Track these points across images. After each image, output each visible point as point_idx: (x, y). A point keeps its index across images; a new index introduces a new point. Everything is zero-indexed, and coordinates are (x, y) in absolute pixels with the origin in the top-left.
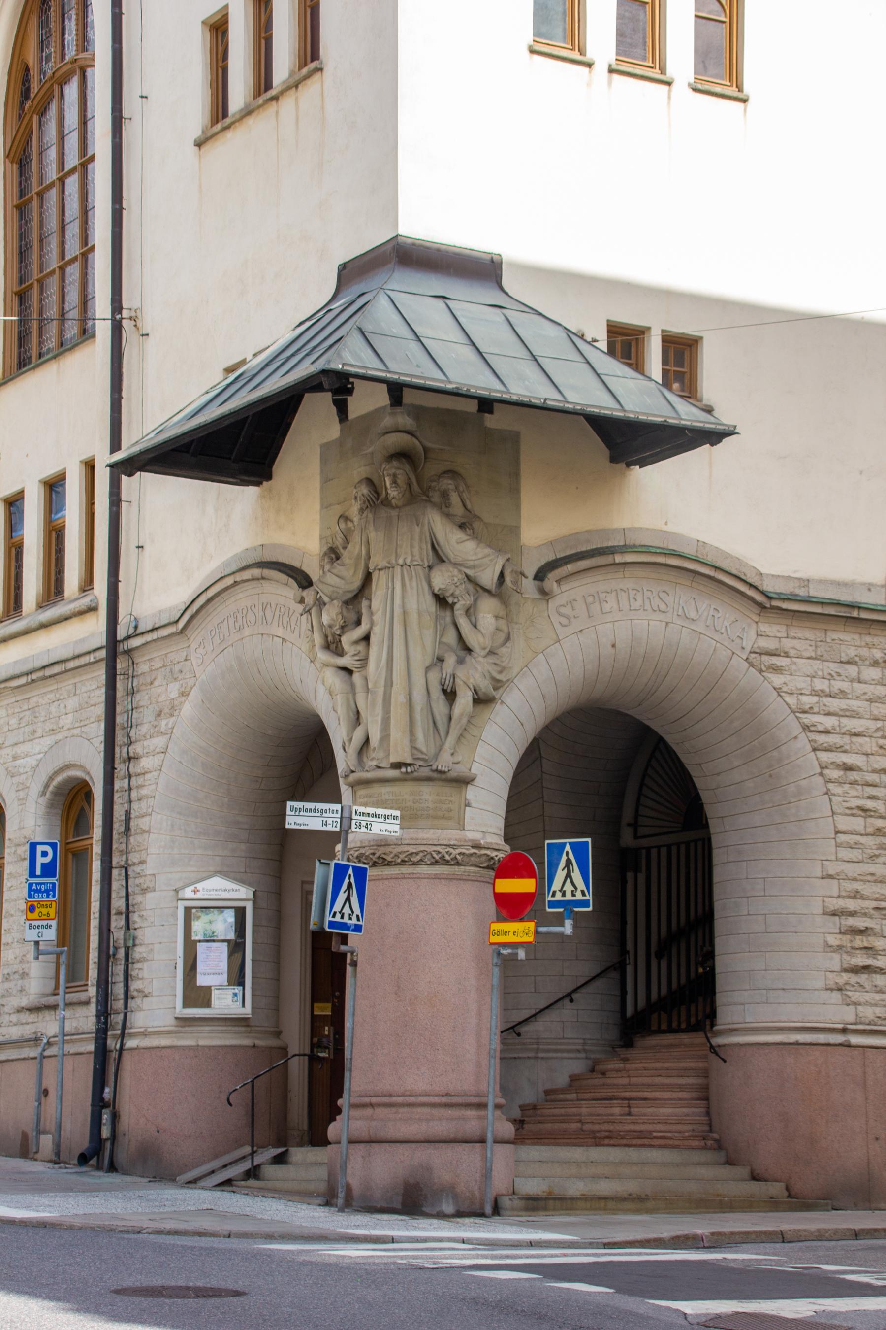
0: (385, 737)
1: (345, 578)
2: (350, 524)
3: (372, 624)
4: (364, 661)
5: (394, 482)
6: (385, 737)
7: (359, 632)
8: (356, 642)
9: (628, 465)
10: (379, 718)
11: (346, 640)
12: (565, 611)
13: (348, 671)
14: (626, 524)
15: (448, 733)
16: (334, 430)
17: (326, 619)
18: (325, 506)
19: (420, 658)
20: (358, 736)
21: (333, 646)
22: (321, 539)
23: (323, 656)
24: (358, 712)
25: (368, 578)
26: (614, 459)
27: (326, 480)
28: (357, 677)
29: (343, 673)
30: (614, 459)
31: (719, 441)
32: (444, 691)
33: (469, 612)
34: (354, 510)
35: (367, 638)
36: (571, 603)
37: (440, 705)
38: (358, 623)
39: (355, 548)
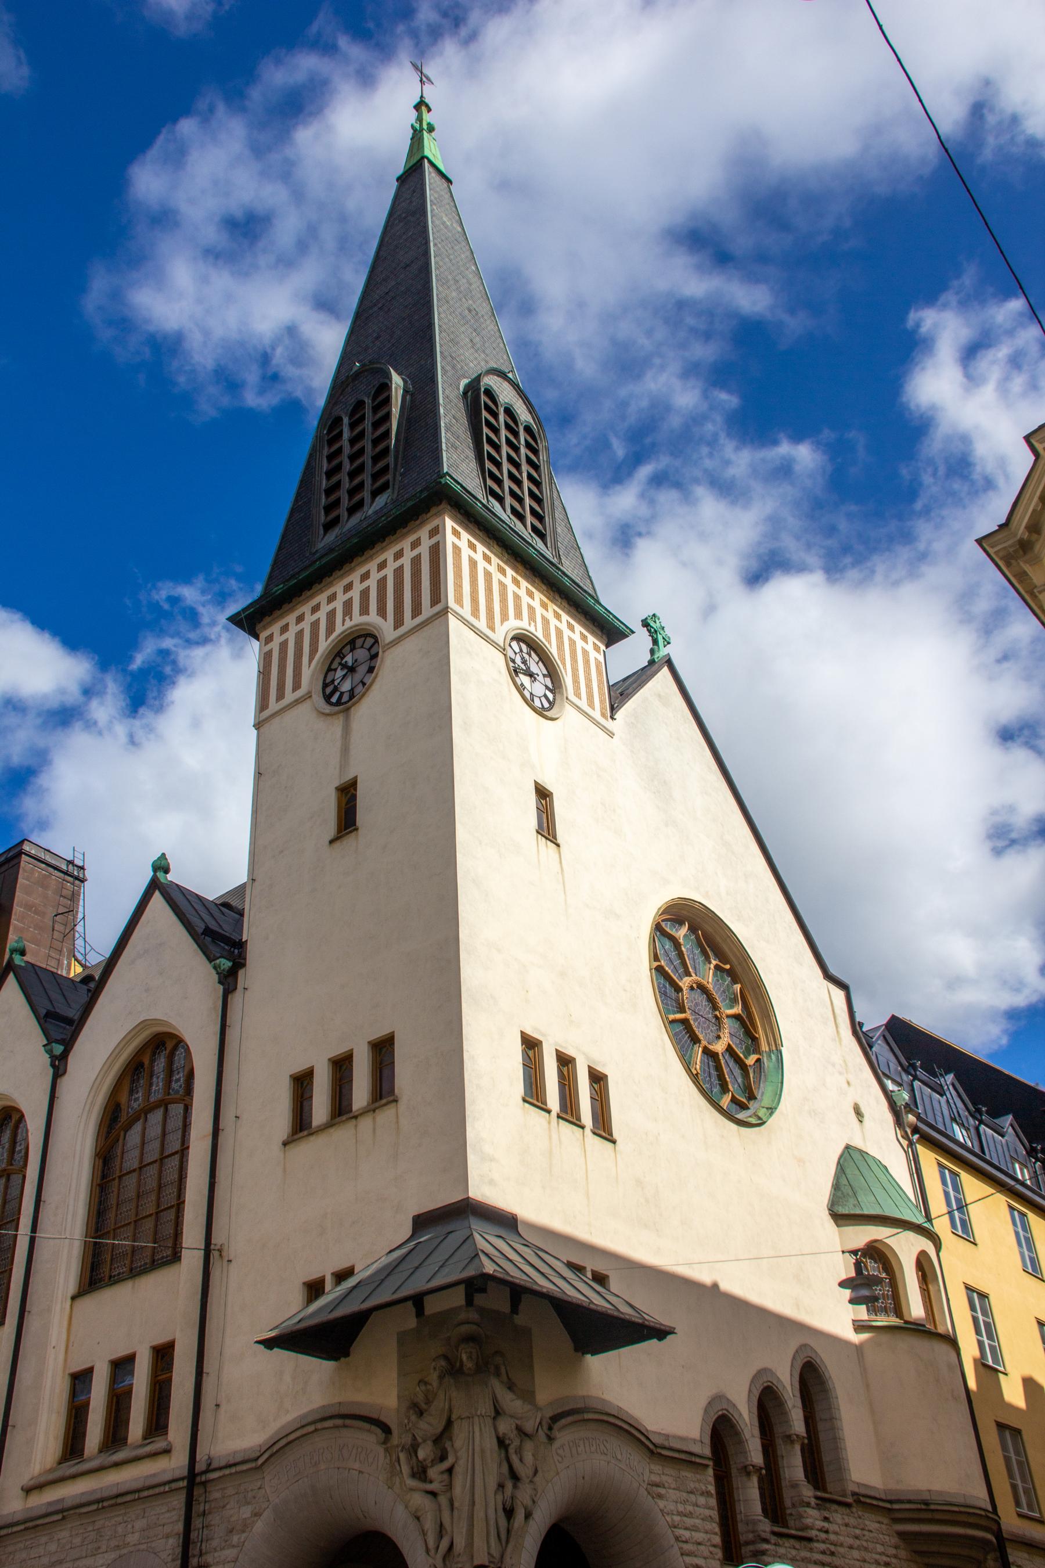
0: (470, 1544)
1: (430, 1425)
2: (429, 1387)
3: (457, 1459)
4: (450, 1486)
5: (470, 1357)
6: (470, 1544)
7: (446, 1465)
8: (442, 1473)
9: (583, 1354)
10: (464, 1530)
11: (433, 1473)
12: (560, 1452)
13: (434, 1494)
14: (585, 1393)
15: (507, 1541)
16: (412, 1322)
17: (421, 1454)
18: (402, 1374)
19: (492, 1485)
20: (444, 1544)
21: (420, 1473)
22: (399, 1397)
23: (411, 1483)
24: (441, 1525)
25: (449, 1423)
26: (576, 1350)
27: (402, 1357)
28: (443, 1500)
29: (429, 1496)
30: (576, 1350)
31: (665, 1337)
32: (504, 1509)
33: (519, 1451)
34: (433, 1377)
35: (450, 1471)
36: (562, 1446)
37: (503, 1522)
38: (443, 1458)
39: (439, 1404)
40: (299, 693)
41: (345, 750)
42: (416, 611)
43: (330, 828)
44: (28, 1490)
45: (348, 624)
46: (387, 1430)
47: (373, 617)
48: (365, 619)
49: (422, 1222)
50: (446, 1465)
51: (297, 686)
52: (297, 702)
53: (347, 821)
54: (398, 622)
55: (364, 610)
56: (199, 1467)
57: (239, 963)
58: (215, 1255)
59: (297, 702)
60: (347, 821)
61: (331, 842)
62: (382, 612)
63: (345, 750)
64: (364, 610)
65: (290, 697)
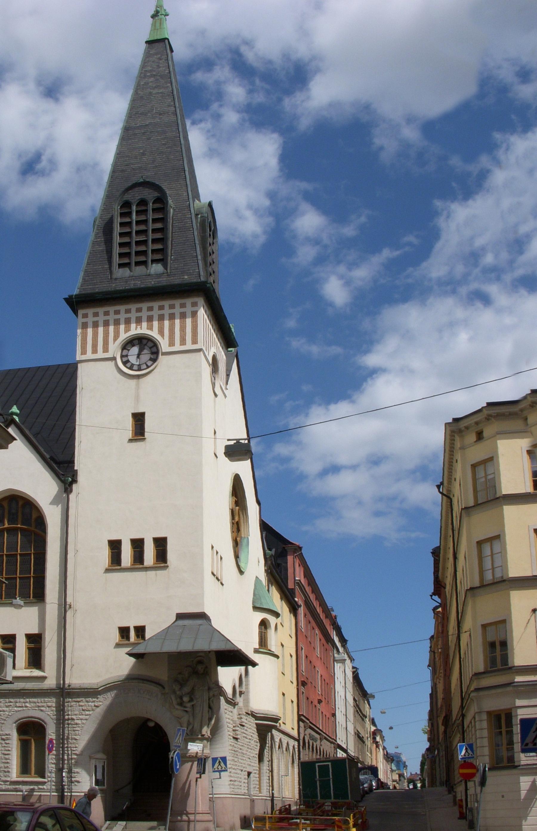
7: (193, 703)
40: (106, 355)
48: (149, 332)
49: (180, 616)
50: (193, 703)
51: (106, 349)
65: (100, 354)
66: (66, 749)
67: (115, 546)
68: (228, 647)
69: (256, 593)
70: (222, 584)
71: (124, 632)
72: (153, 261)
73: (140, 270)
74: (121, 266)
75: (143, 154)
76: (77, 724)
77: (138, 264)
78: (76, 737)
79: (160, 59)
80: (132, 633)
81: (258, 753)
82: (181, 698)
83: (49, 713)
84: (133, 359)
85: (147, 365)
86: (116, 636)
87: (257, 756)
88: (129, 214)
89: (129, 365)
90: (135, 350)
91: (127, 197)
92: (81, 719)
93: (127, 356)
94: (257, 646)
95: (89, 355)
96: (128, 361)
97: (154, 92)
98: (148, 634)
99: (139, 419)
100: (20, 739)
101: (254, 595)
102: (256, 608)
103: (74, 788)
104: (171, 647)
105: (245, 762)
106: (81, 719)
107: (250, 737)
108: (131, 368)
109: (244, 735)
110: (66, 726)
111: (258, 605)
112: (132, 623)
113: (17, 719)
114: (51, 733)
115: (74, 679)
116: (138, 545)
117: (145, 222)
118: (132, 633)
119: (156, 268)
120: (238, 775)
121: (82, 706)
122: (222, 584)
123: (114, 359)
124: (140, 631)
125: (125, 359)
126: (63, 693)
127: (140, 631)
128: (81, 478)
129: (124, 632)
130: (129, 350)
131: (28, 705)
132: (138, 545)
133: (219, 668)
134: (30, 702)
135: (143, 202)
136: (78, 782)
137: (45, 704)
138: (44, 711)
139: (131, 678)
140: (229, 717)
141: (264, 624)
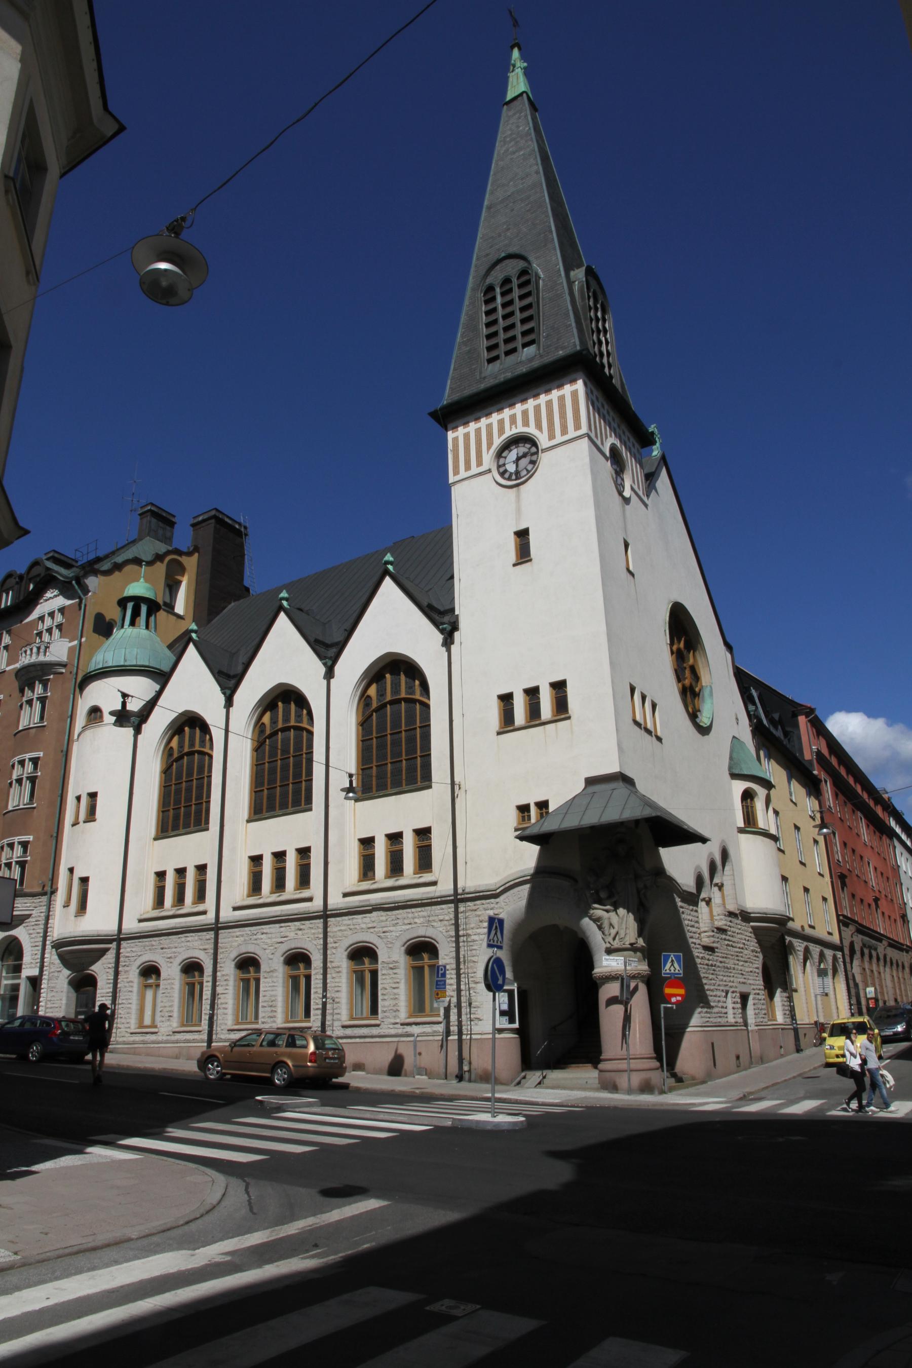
40: (481, 469)
41: (518, 510)
42: (564, 431)
43: (512, 556)
44: (346, 895)
45: (515, 431)
46: (576, 881)
47: (532, 430)
49: (590, 781)
51: (480, 463)
52: (480, 474)
53: (523, 553)
54: (552, 436)
55: (526, 423)
56: (460, 891)
57: (455, 627)
58: (457, 787)
59: (480, 474)
60: (523, 553)
61: (514, 565)
62: (539, 426)
63: (518, 510)
64: (526, 423)
65: (475, 470)
66: (463, 976)
67: (506, 699)
68: (648, 812)
69: (735, 755)
70: (659, 739)
71: (524, 809)
72: (525, 345)
73: (512, 358)
74: (490, 361)
75: (509, 229)
76: (474, 941)
77: (507, 353)
78: (473, 959)
79: (519, 118)
80: (533, 810)
81: (760, 966)
82: (597, 892)
83: (441, 929)
84: (511, 468)
85: (528, 472)
86: (512, 818)
87: (760, 971)
88: (494, 299)
89: (507, 475)
90: (513, 455)
91: (489, 281)
92: (479, 934)
93: (504, 465)
94: (741, 824)
95: (463, 474)
96: (506, 471)
97: (515, 156)
98: (552, 808)
99: (523, 535)
100: (413, 967)
101: (731, 758)
102: (734, 776)
103: (476, 1029)
104: (571, 822)
105: (732, 979)
106: (479, 934)
107: (742, 946)
108: (509, 479)
109: (727, 942)
110: (461, 944)
111: (737, 772)
112: (531, 799)
113: (405, 940)
114: (446, 956)
115: (470, 882)
116: (532, 693)
117: (511, 303)
118: (533, 810)
119: (531, 350)
120: (717, 999)
121: (479, 916)
122: (659, 739)
123: (489, 471)
124: (543, 805)
125: (502, 470)
126: (457, 899)
127: (543, 805)
128: (462, 624)
129: (524, 809)
130: (505, 458)
131: (416, 920)
132: (532, 693)
133: (664, 852)
134: (419, 917)
135: (507, 281)
136: (480, 1020)
137: (436, 918)
138: (435, 926)
139: (542, 873)
140: (690, 918)
141: (748, 796)
